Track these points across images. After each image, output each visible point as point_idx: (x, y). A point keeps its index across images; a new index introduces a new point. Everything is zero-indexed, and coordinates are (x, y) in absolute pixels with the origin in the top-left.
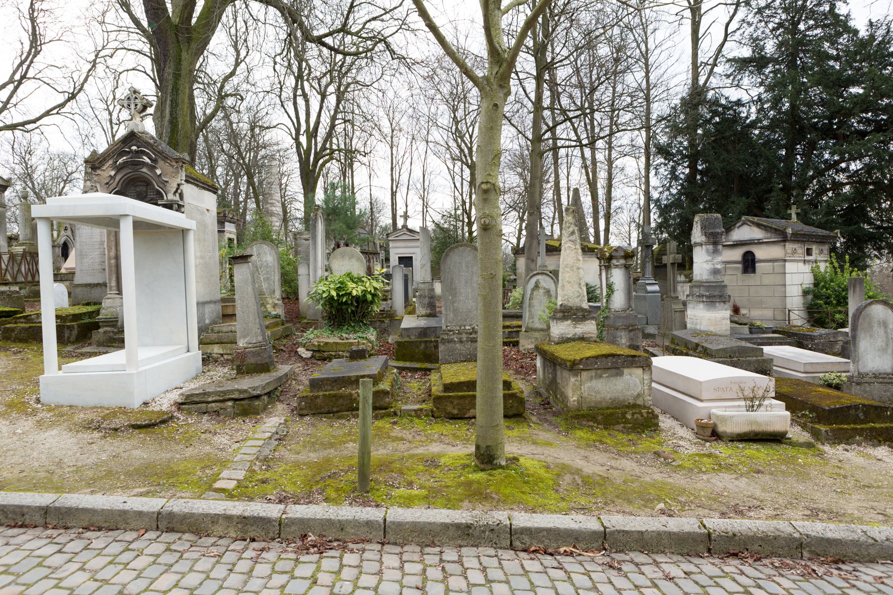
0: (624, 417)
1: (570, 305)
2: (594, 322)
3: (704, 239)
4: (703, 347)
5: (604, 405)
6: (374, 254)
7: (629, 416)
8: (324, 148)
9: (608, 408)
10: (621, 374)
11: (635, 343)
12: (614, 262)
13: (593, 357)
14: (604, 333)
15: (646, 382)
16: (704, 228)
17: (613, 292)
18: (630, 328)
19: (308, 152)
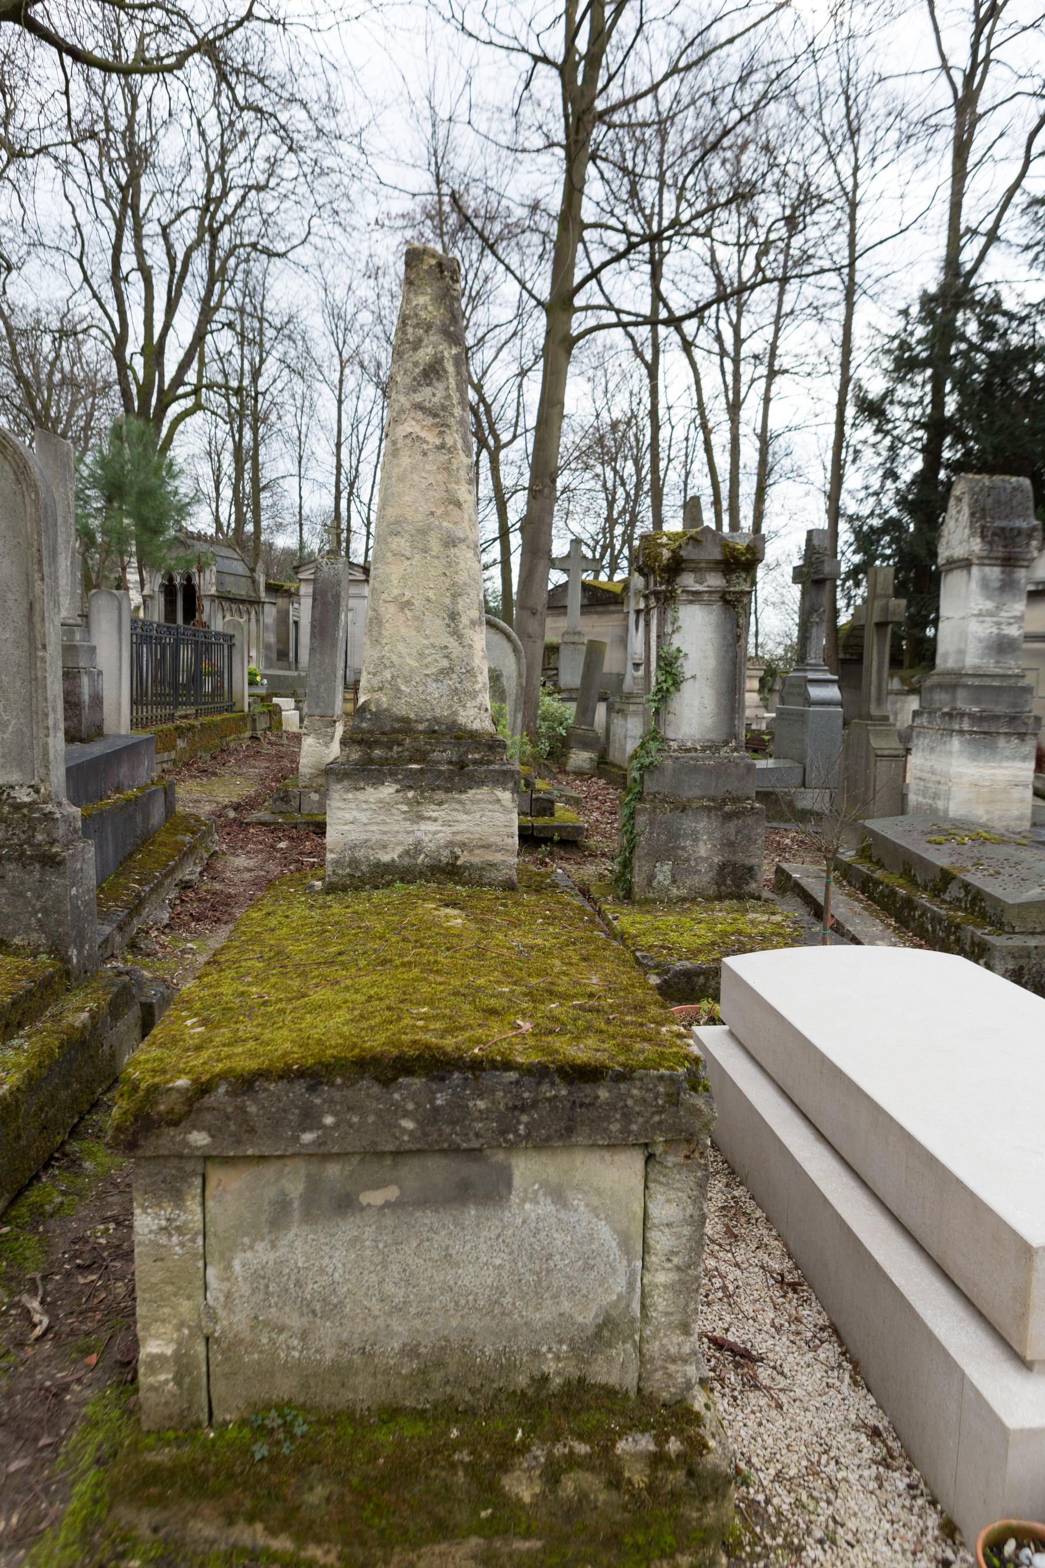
0: (487, 1485)
1: (401, 709)
2: (506, 796)
3: (976, 545)
4: (966, 886)
5: (363, 1392)
6: (252, 603)
7: (522, 1487)
8: (178, 380)
9: (391, 1413)
10: (495, 1191)
11: (740, 858)
12: (688, 580)
13: (287, 1074)
14: (641, 819)
15: (662, 1241)
16: (979, 513)
17: (677, 684)
18: (726, 809)
19: (145, 391)
